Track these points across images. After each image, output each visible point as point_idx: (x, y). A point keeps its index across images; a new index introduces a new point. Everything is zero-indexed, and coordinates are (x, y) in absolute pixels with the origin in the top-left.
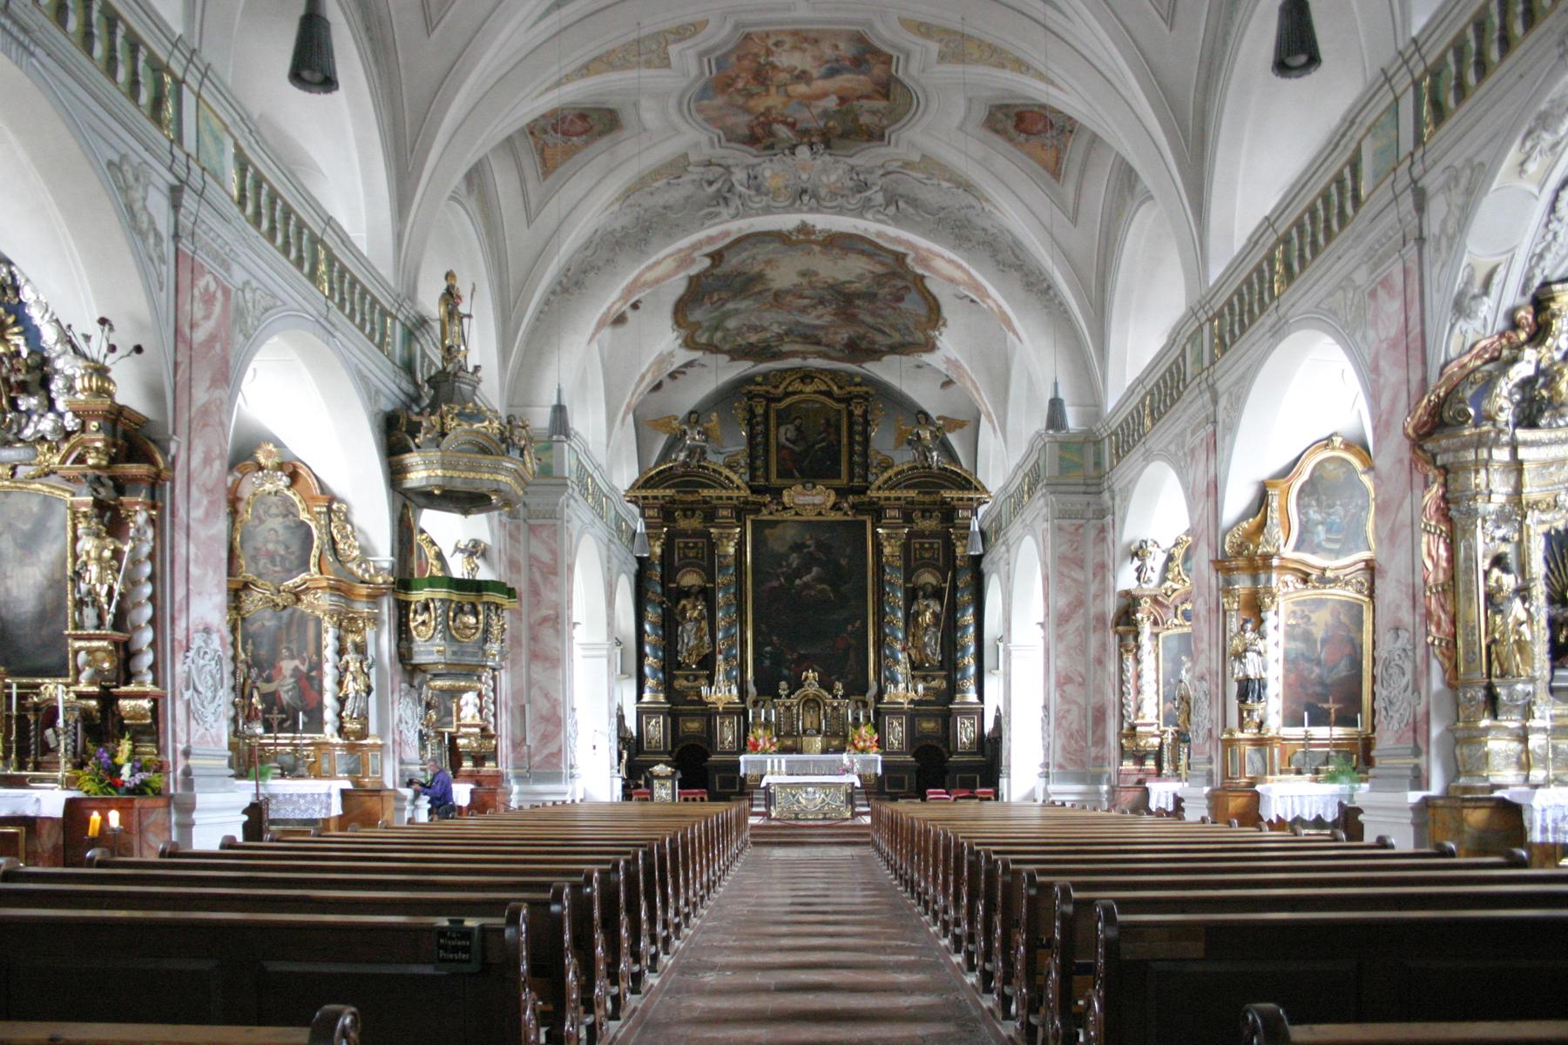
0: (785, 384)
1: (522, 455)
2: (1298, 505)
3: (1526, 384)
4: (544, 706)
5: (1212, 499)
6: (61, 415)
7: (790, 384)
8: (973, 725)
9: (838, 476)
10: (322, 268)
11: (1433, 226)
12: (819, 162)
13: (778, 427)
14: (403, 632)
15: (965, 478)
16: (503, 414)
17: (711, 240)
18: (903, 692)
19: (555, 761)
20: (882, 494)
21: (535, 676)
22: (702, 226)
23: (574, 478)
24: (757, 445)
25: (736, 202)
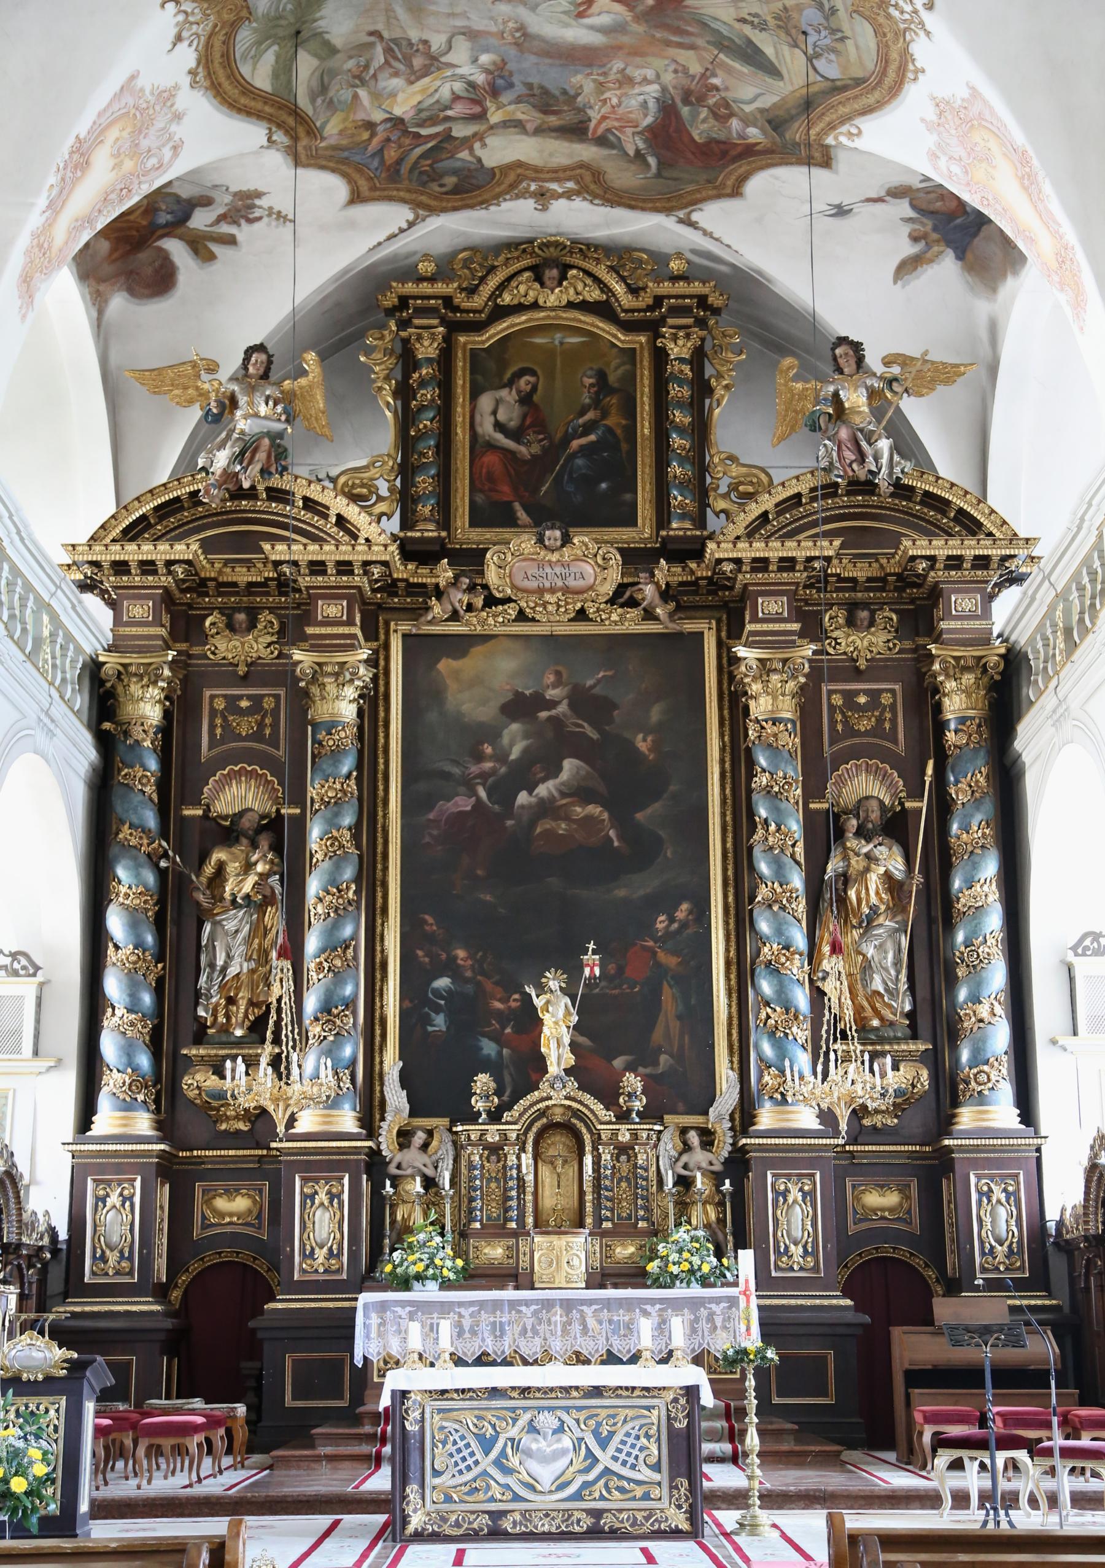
0: (493, 282)
7: (502, 287)
9: (630, 520)
13: (475, 393)
24: (422, 436)
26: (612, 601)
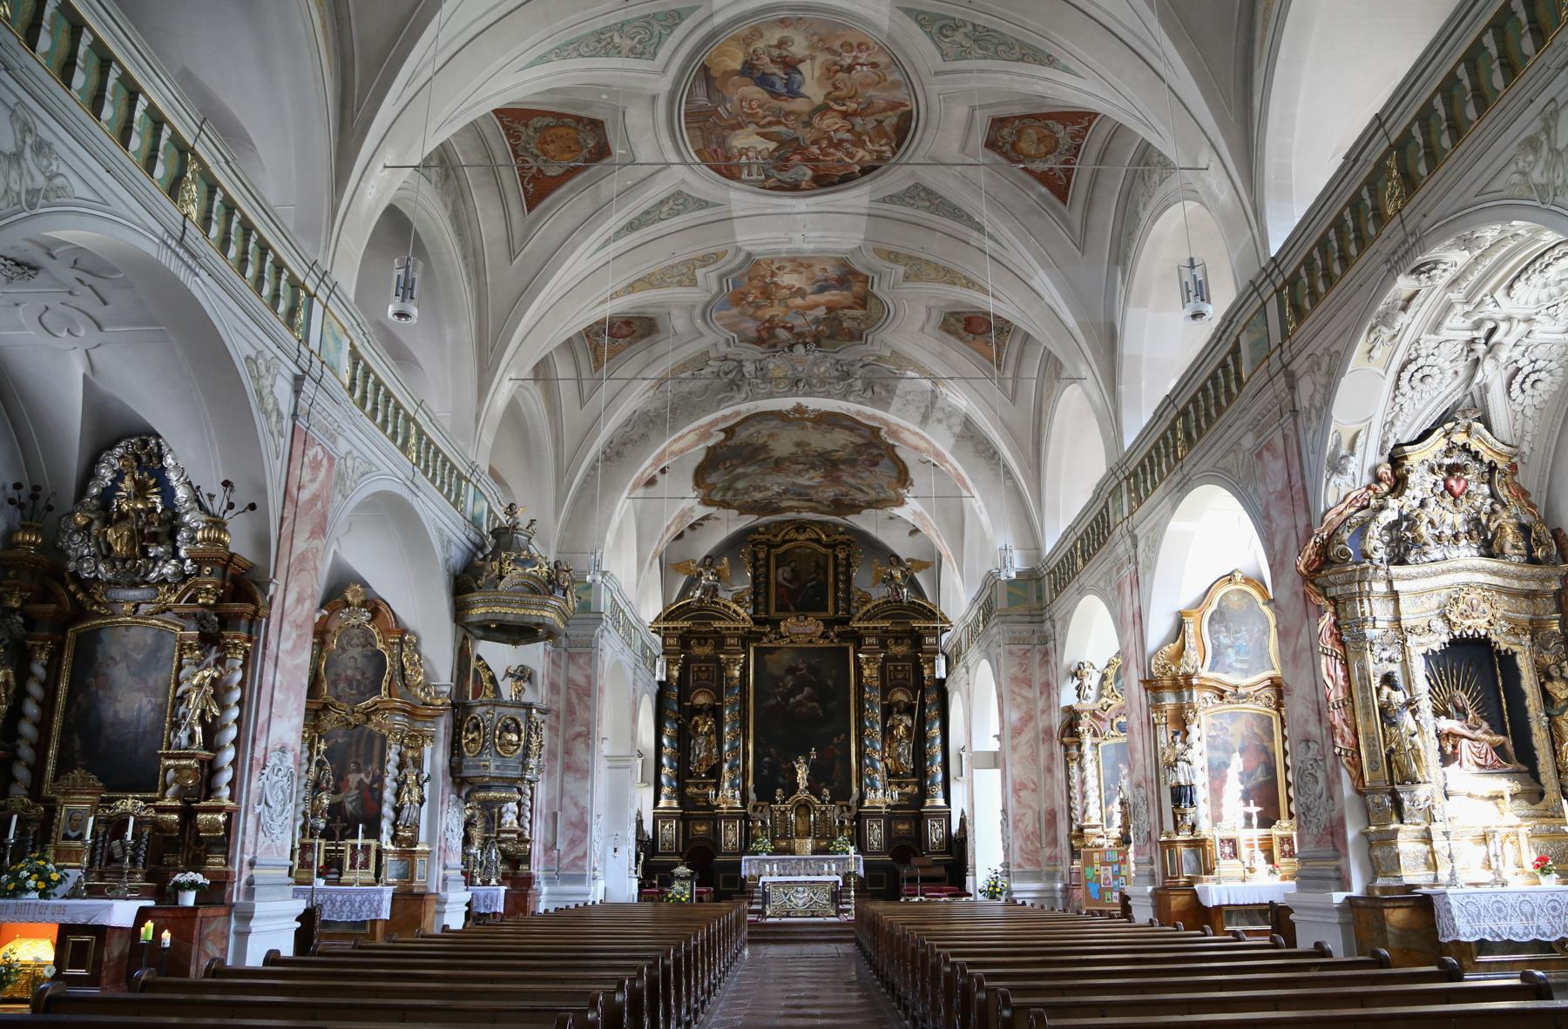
1: (565, 595)
2: (1210, 631)
3: (1393, 526)
4: (573, 813)
5: (1137, 627)
6: (182, 561)
8: (941, 826)
10: (413, 441)
11: (1303, 401)
12: (811, 357)
14: (455, 747)
15: (930, 610)
16: (552, 559)
17: (725, 418)
18: (880, 797)
19: (580, 863)
20: (862, 625)
21: (567, 786)
22: (718, 408)
23: (608, 612)
25: (746, 388)
26: (821, 637)
